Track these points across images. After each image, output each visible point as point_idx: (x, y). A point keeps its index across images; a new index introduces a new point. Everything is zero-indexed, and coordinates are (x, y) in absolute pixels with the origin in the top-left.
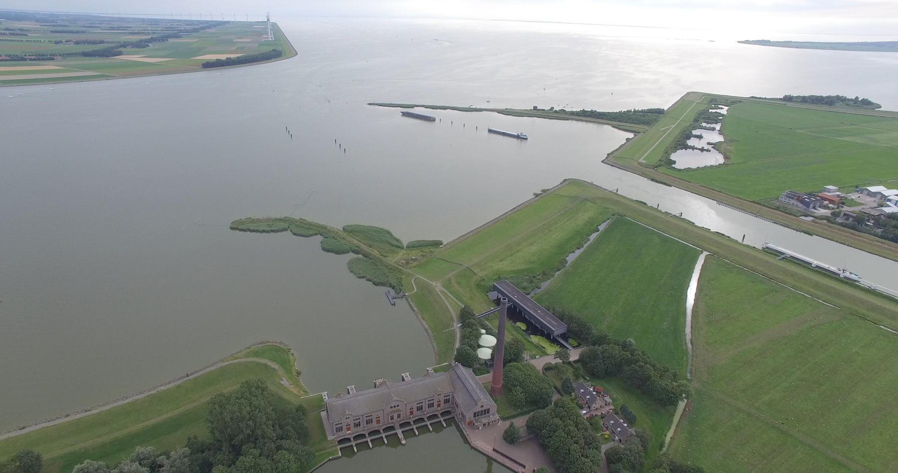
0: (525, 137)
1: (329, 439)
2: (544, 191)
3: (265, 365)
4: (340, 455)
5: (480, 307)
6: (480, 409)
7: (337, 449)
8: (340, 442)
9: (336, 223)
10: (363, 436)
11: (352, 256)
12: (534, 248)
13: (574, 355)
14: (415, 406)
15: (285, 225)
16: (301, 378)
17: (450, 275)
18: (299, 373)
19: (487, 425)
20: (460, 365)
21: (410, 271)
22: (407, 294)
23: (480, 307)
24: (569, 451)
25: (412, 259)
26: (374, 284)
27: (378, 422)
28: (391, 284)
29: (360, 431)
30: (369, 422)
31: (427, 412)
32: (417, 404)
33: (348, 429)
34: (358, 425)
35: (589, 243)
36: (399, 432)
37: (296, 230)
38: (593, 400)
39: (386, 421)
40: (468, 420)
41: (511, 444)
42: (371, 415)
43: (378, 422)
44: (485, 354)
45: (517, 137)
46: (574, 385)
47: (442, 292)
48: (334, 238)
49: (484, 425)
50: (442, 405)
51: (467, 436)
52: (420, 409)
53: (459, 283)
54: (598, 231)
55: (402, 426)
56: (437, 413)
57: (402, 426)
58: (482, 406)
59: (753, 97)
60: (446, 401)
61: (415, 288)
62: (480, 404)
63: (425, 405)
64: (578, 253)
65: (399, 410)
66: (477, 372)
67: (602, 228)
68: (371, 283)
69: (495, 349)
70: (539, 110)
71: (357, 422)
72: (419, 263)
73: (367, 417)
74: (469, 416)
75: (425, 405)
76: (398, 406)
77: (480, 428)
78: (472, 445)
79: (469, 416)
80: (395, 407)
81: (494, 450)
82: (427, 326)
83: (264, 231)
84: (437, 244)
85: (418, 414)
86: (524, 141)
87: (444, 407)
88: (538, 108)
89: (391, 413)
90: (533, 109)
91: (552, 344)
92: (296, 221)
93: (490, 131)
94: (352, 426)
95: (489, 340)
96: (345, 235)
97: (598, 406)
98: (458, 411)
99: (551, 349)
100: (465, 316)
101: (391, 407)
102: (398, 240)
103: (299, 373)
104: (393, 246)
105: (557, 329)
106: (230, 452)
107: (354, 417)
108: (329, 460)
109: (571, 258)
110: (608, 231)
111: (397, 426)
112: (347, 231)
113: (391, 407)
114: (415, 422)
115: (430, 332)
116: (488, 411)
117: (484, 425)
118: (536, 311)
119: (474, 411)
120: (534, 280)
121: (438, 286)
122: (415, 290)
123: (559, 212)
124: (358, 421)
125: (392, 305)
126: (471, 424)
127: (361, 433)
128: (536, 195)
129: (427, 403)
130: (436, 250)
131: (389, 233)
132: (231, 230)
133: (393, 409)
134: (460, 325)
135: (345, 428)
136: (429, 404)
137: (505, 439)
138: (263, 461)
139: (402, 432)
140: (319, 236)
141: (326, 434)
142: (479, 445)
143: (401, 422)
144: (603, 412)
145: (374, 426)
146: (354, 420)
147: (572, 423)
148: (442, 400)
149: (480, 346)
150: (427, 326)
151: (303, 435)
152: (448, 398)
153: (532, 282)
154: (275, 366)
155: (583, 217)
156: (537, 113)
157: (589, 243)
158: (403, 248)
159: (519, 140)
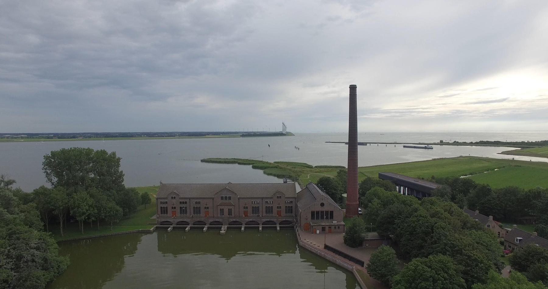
6: (320, 209)
24: (432, 230)
42: (199, 203)
45: (425, 148)
56: (275, 220)
60: (289, 210)
65: (231, 205)
70: (445, 143)
76: (230, 198)
77: (318, 232)
85: (252, 217)
88: (444, 142)
89: (221, 205)
101: (222, 198)
116: (330, 215)
117: (323, 229)
122: (308, 178)
124: (184, 205)
127: (185, 220)
129: (265, 205)
133: (224, 201)
142: (309, 243)
145: (202, 217)
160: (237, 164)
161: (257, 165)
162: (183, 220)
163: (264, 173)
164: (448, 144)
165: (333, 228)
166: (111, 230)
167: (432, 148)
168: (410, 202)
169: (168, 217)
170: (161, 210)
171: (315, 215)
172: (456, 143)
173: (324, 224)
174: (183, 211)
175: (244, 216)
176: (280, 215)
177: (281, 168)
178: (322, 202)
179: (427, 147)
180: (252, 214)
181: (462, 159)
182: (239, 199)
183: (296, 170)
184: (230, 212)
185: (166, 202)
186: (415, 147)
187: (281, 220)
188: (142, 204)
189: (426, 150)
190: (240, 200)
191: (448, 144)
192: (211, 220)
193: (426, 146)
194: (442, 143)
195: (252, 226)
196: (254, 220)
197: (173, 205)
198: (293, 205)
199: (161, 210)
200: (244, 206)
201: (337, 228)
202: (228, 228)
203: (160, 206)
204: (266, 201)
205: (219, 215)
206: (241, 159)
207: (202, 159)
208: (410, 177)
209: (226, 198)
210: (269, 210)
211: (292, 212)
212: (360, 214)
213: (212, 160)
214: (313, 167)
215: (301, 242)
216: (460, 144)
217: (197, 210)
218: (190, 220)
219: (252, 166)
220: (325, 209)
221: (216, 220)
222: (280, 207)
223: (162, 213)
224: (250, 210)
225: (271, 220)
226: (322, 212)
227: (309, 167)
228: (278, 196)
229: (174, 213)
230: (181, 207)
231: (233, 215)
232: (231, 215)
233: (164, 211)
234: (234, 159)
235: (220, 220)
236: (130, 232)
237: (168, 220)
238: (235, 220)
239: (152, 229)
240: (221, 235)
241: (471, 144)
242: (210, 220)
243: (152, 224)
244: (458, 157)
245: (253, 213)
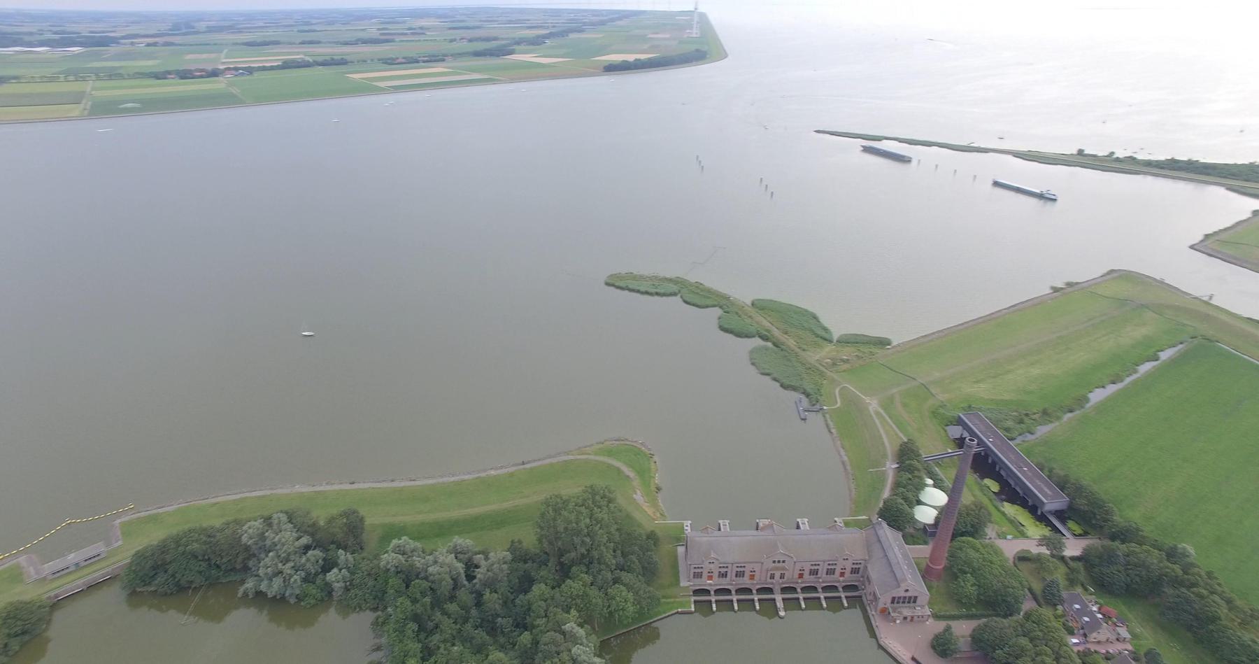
0: (1054, 197)
1: (682, 585)
2: (1069, 284)
3: (618, 469)
4: (693, 609)
5: (933, 444)
6: (903, 594)
7: (690, 601)
8: (696, 592)
9: (744, 294)
10: (728, 591)
11: (757, 342)
12: (1035, 371)
13: (1073, 548)
14: (807, 568)
15: (675, 288)
16: (660, 496)
17: (895, 391)
18: (659, 489)
19: (909, 619)
20: (884, 525)
21: (835, 376)
22: (825, 408)
23: (933, 444)
25: (843, 360)
26: (782, 385)
27: (752, 577)
28: (805, 390)
29: (724, 583)
30: (739, 574)
31: (823, 579)
32: (812, 565)
33: (710, 578)
34: (724, 575)
35: (1134, 377)
36: (779, 598)
37: (689, 297)
38: (1095, 625)
39: (763, 579)
40: (881, 605)
41: (942, 657)
42: (744, 567)
43: (752, 577)
44: (925, 515)
45: (1041, 196)
46: (1064, 594)
47: (877, 413)
48: (737, 313)
49: (905, 618)
50: (848, 574)
51: (876, 629)
52: (814, 572)
53: (905, 405)
54: (1157, 360)
55: (784, 590)
57: (784, 590)
58: (907, 591)
61: (839, 400)
62: (904, 586)
63: (822, 569)
64: (1112, 389)
65: (784, 569)
66: (909, 539)
67: (1164, 356)
68: (778, 384)
69: (944, 512)
71: (723, 570)
72: (852, 366)
73: (737, 567)
74: (884, 601)
75: (822, 569)
76: (784, 562)
77: (898, 622)
78: (882, 643)
79: (884, 601)
80: (779, 562)
82: (846, 458)
83: (647, 293)
84: (883, 343)
85: (809, 580)
86: (1049, 203)
87: (849, 578)
91: (1038, 523)
92: (691, 284)
93: (996, 184)
94: (716, 575)
95: (935, 497)
96: (752, 312)
97: (1102, 637)
98: (869, 589)
99: (1035, 531)
100: (906, 455)
101: (774, 562)
102: (826, 329)
103: (659, 489)
104: (817, 336)
105: (1052, 501)
106: (556, 571)
107: (721, 563)
108: (678, 613)
109: (1097, 396)
110: (1173, 362)
111: (777, 589)
112: (757, 308)
113: (774, 562)
114: (804, 589)
115: (849, 468)
118: (1020, 468)
119: (894, 596)
120: (1026, 420)
121: (873, 404)
123: (1090, 320)
124: (726, 570)
125: (803, 419)
126: (885, 612)
127: (726, 587)
128: (1056, 290)
130: (879, 351)
131: (815, 317)
132: (607, 287)
133: (777, 564)
134: (897, 466)
135: (705, 575)
136: (828, 569)
137: (933, 647)
138: (593, 592)
139: (783, 599)
140: (717, 308)
141: (679, 577)
143: (784, 586)
144: (1111, 651)
145: (745, 582)
146: (720, 567)
147: (1049, 651)
148: (849, 566)
149: (919, 503)
150: (846, 458)
151: (649, 572)
152: (857, 566)
153: (1021, 422)
154: (632, 475)
155: (1134, 333)
156: (1082, 160)
157: (1134, 377)
158: (831, 341)
159: (1042, 201)
165: (915, 617)
198: (861, 566)
203: (693, 571)
210: (830, 572)
211: (858, 573)
220: (908, 594)
226: (905, 598)
240: (780, 617)
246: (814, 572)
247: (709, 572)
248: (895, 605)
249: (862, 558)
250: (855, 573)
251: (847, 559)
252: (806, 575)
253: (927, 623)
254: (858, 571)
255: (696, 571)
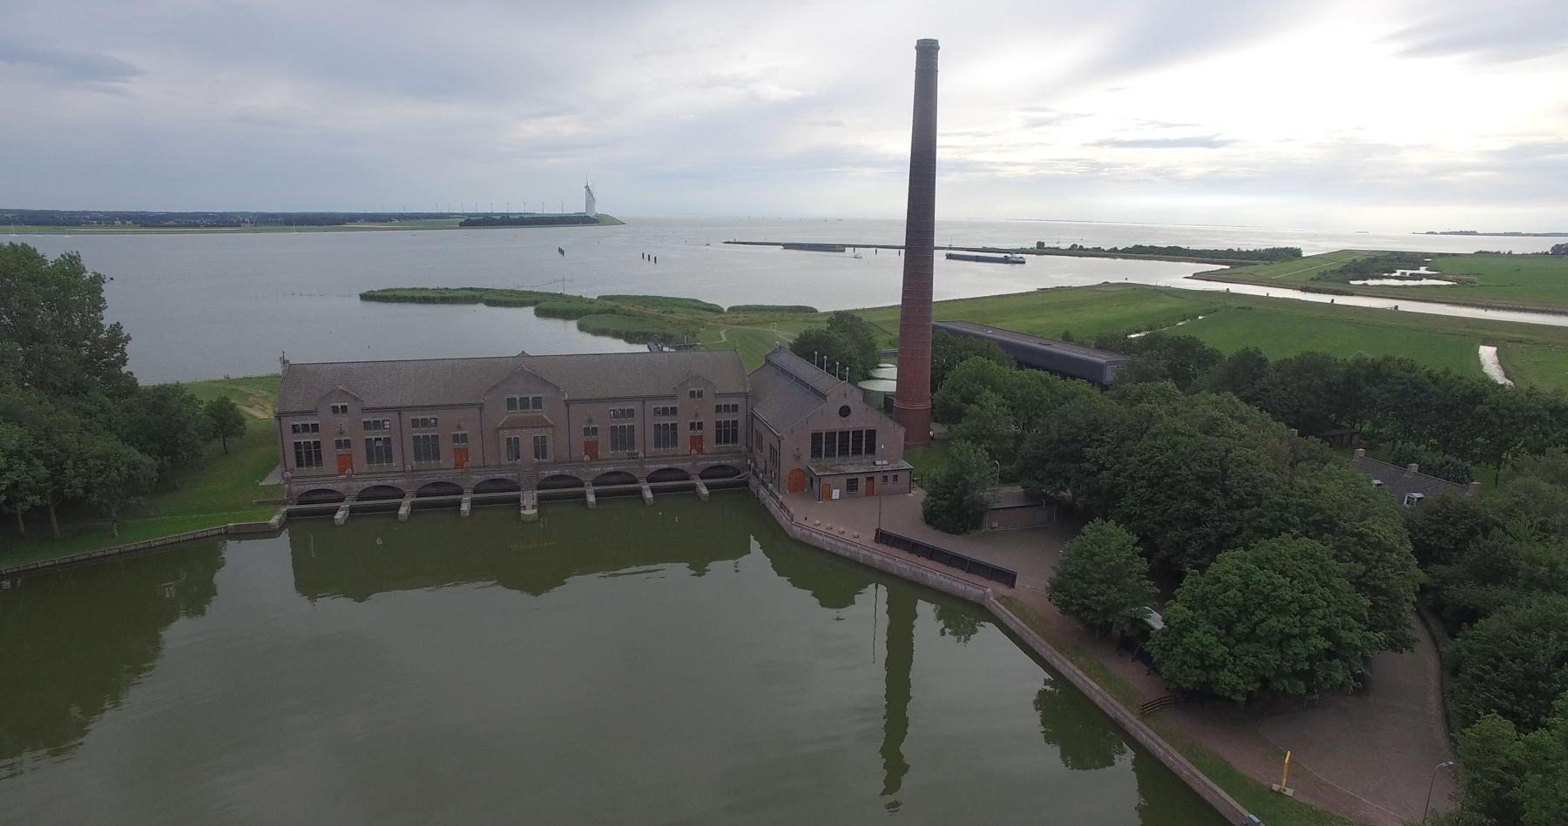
6: (837, 424)
27: (462, 455)
30: (427, 448)
41: (958, 533)
43: (462, 455)
45: (1006, 261)
52: (623, 438)
56: (686, 466)
58: (845, 412)
59: (1481, 252)
60: (726, 433)
63: (645, 426)
65: (540, 424)
74: (795, 452)
76: (537, 403)
77: (836, 494)
78: (796, 531)
79: (795, 452)
81: (883, 537)
85: (611, 460)
89: (511, 425)
90: (1035, 246)
101: (511, 403)
116: (864, 442)
117: (852, 485)
119: (816, 429)
127: (389, 482)
133: (518, 413)
135: (330, 455)
136: (657, 427)
145: (444, 468)
148: (710, 421)
152: (729, 417)
160: (481, 307)
161: (551, 307)
162: (380, 483)
163: (581, 328)
164: (1057, 252)
165: (878, 479)
166: (113, 536)
167: (1024, 263)
168: (1089, 397)
169: (326, 476)
170: (297, 453)
171: (824, 444)
172: (1076, 251)
173: (852, 470)
174: (379, 452)
175: (587, 458)
176: (700, 451)
177: (628, 314)
178: (844, 403)
179: (1010, 258)
180: (611, 452)
181: (1108, 289)
182: (567, 403)
183: (679, 318)
184: (540, 449)
185: (315, 428)
186: (977, 259)
187: (703, 464)
188: (216, 436)
189: (1008, 265)
190: (573, 408)
191: (1057, 252)
192: (477, 478)
193: (1009, 255)
194: (1041, 249)
195: (619, 489)
196: (619, 468)
197: (342, 433)
198: (740, 416)
199: (298, 455)
200: (585, 426)
201: (890, 477)
202: (540, 498)
203: (291, 439)
204: (654, 407)
205: (505, 461)
206: (493, 291)
207: (364, 291)
208: (1011, 331)
209: (524, 403)
210: (667, 435)
211: (735, 440)
212: (932, 438)
213: (398, 293)
214: (722, 309)
215: (794, 528)
216: (1086, 252)
217: (427, 448)
218: (405, 480)
219: (536, 310)
220: (852, 424)
221: (498, 476)
222: (700, 425)
223: (299, 464)
224: (604, 439)
225: (675, 465)
226: (844, 434)
227: (711, 310)
228: (692, 389)
229: (345, 463)
230: (368, 441)
231: (551, 457)
232: (544, 456)
233: (309, 455)
234: (471, 289)
235: (509, 475)
236: (192, 537)
237: (325, 486)
238: (557, 472)
239: (275, 520)
241: (1114, 253)
242: (474, 477)
243: (274, 503)
244: (1099, 286)
245: (614, 447)
246: (623, 438)
247: (339, 444)
248: (824, 461)
249: (740, 390)
250: (726, 441)
251: (700, 394)
252: (605, 451)
253: (910, 495)
254: (735, 432)
255: (303, 438)
